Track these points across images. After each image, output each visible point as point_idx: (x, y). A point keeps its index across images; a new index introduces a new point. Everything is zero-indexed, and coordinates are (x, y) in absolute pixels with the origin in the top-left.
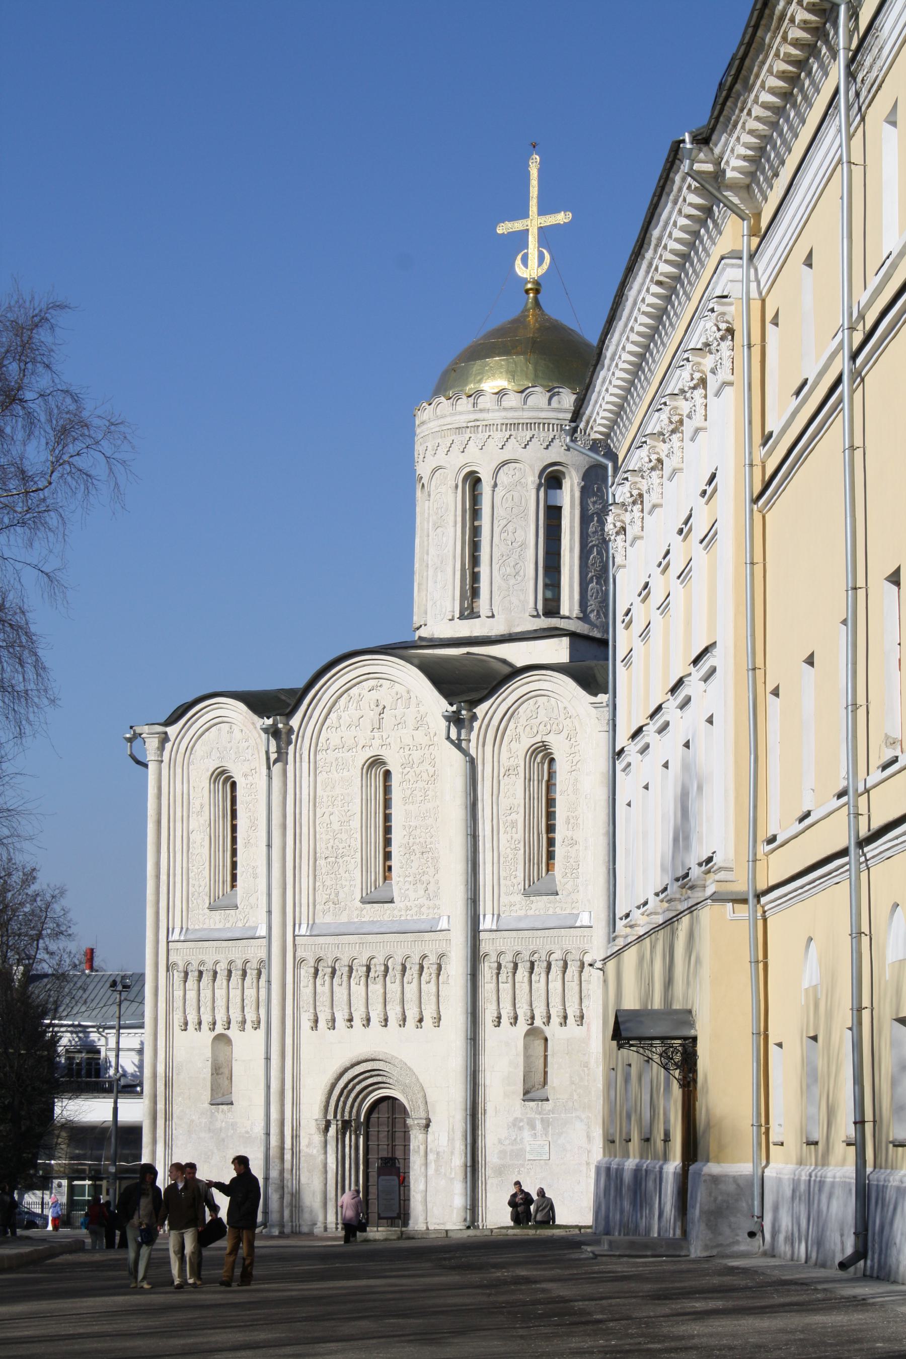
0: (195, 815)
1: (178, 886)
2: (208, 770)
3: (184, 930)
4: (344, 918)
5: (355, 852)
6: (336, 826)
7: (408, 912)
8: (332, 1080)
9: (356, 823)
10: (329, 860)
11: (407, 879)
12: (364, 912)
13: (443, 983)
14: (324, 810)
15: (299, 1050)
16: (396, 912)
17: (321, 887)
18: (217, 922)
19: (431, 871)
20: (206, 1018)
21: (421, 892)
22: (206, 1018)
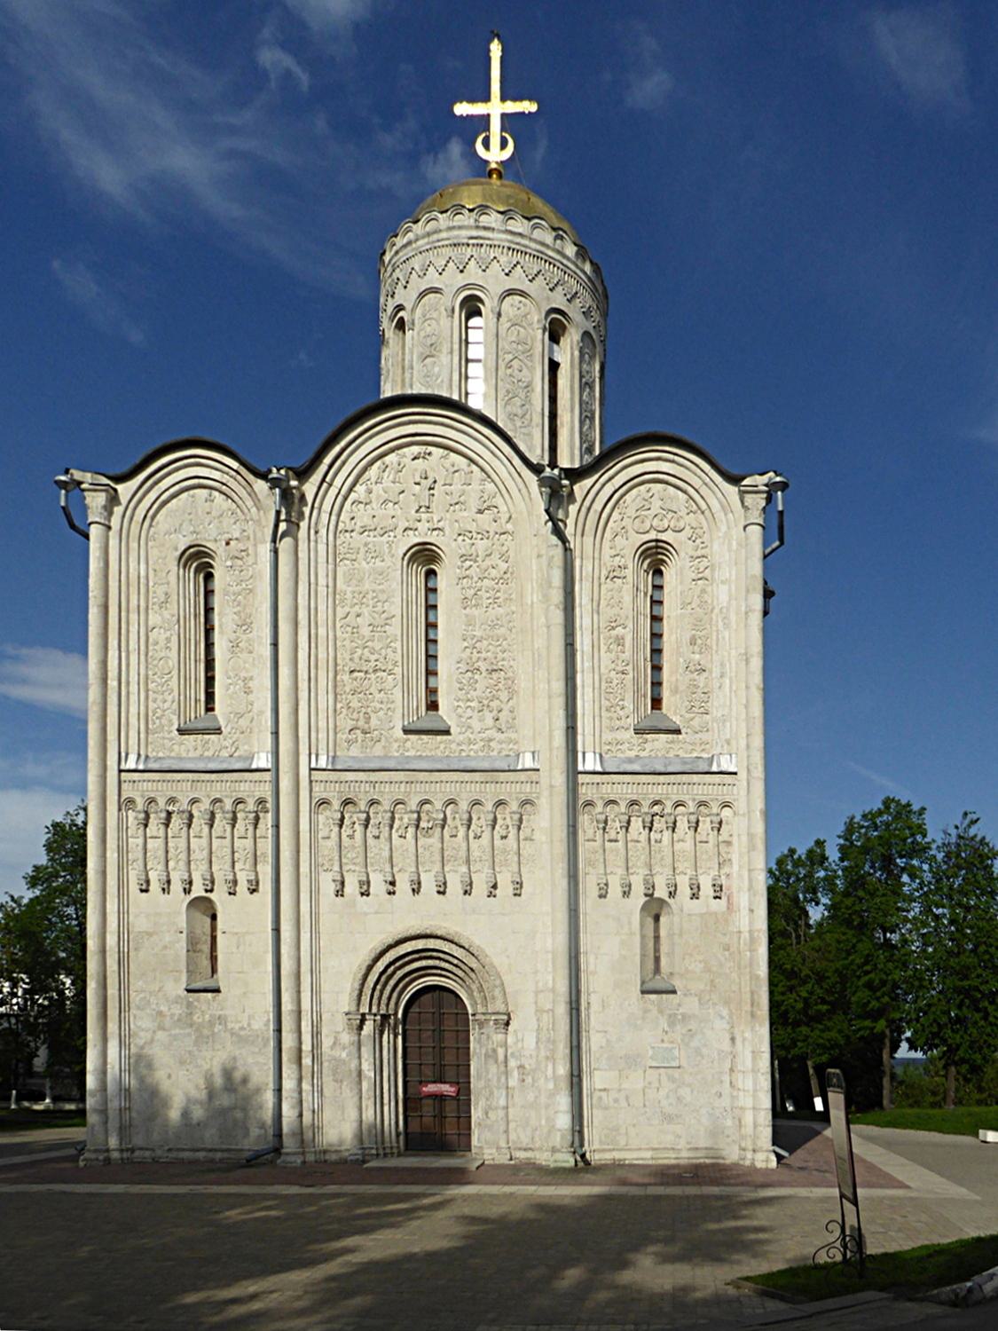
0: (156, 607)
1: (133, 698)
2: (176, 549)
3: (143, 757)
4: (378, 750)
5: (395, 664)
6: (366, 631)
7: (472, 746)
8: (368, 962)
9: (395, 629)
10: (356, 674)
11: (469, 704)
12: (408, 744)
13: (526, 839)
14: (347, 609)
15: (318, 922)
16: (453, 746)
17: (344, 711)
18: (191, 749)
19: (504, 695)
20: (177, 878)
21: (489, 722)
22: (177, 878)
